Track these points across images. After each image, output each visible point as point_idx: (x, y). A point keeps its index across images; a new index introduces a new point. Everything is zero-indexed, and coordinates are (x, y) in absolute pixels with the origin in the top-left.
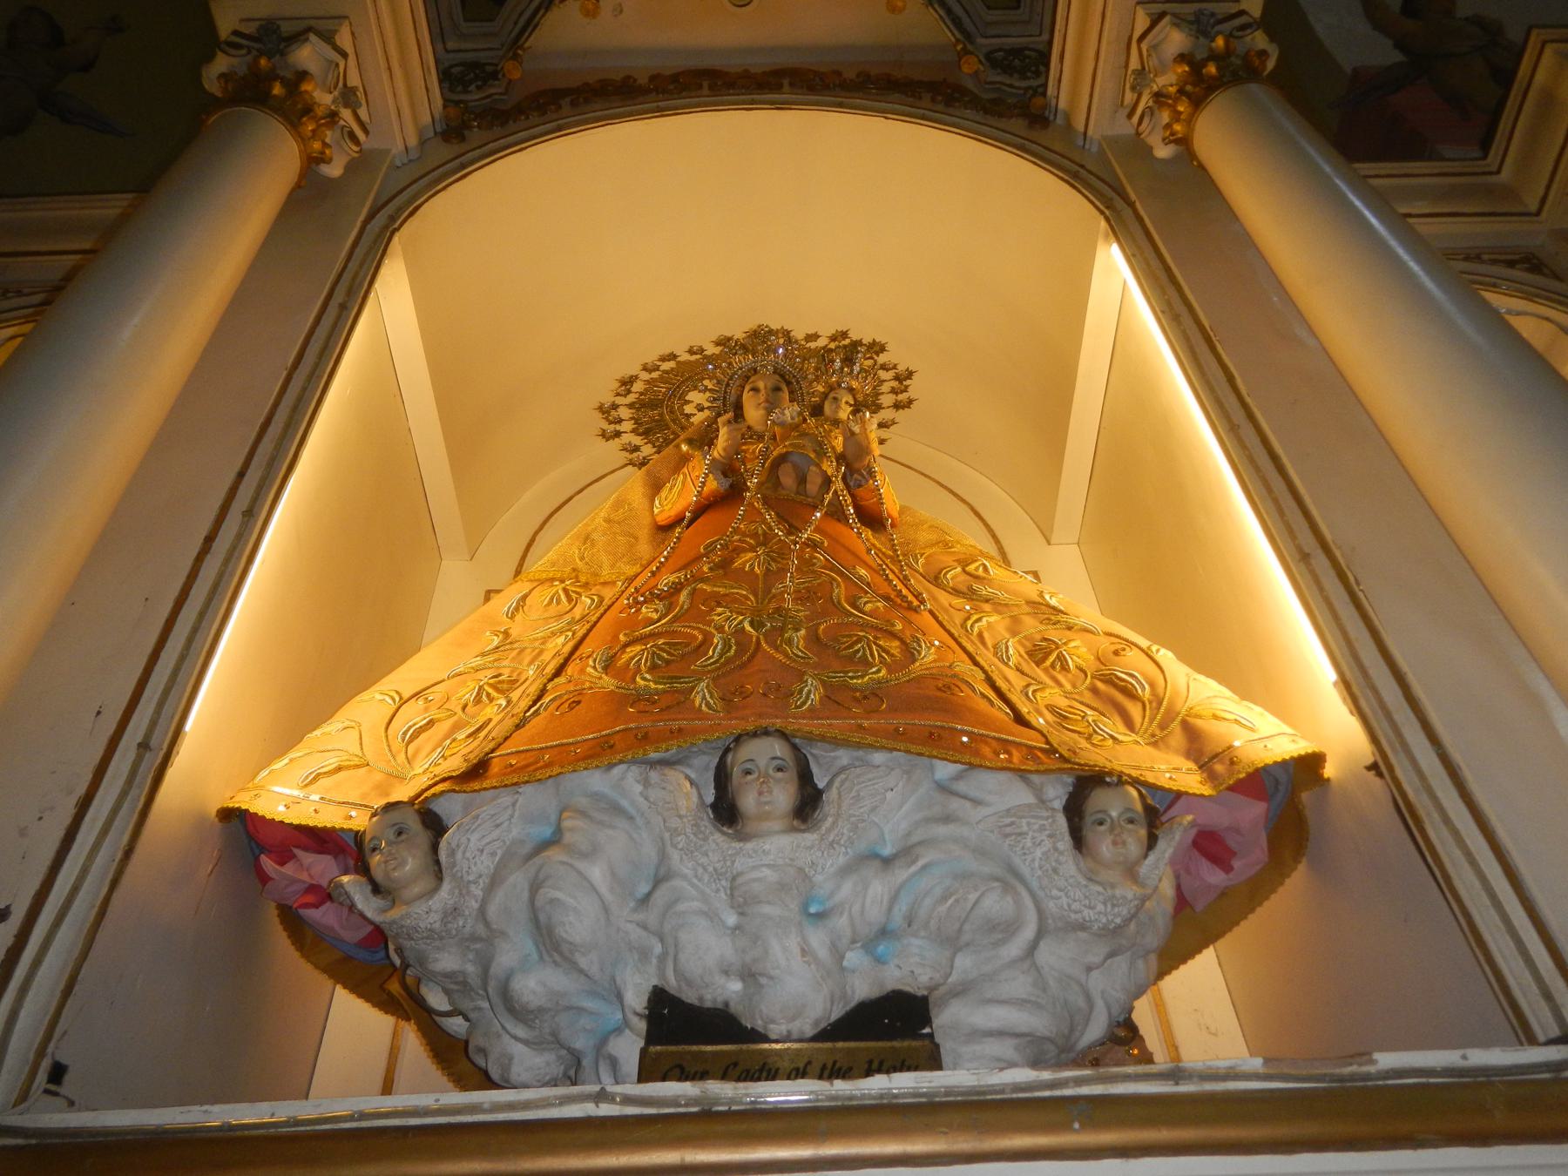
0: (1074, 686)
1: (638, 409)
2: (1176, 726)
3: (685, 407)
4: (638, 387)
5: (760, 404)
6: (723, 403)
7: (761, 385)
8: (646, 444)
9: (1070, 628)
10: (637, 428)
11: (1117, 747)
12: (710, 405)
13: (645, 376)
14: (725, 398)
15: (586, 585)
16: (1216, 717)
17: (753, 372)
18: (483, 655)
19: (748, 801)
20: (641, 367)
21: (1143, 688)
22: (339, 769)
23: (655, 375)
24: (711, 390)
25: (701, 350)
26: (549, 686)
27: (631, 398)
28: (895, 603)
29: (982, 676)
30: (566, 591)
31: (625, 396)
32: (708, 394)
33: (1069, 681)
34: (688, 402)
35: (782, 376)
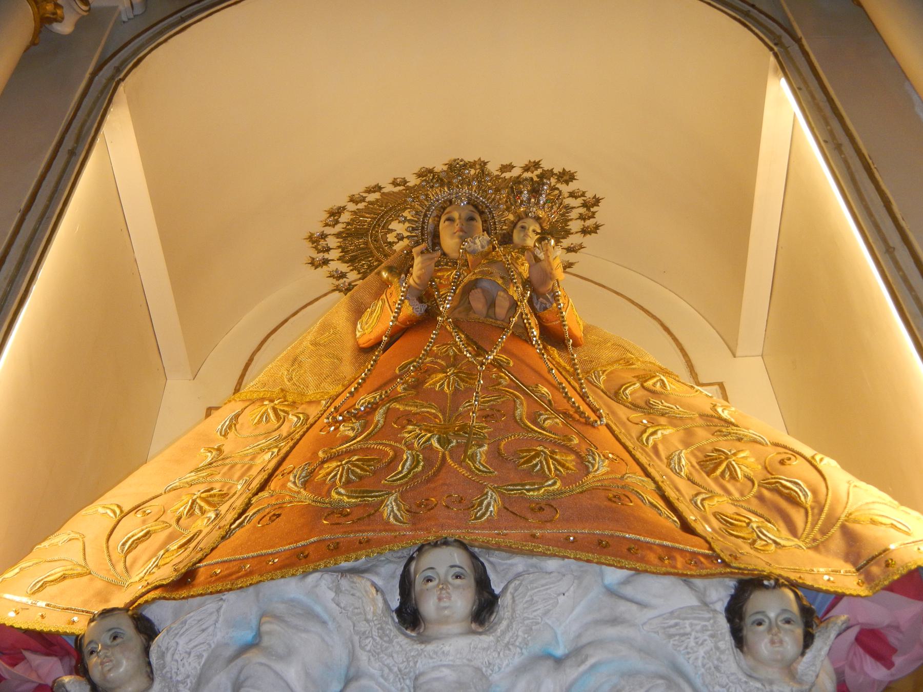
0: (742, 495)
1: (345, 239)
2: (835, 530)
3: (388, 236)
4: (345, 217)
5: (455, 233)
6: (422, 232)
7: (456, 215)
8: (352, 270)
9: (740, 439)
10: (343, 256)
11: (779, 551)
12: (409, 234)
13: (352, 207)
14: (423, 228)
15: (293, 404)
16: (873, 522)
17: (449, 203)
18: (197, 470)
19: (429, 606)
20: (348, 199)
21: (806, 495)
22: (64, 578)
23: (361, 206)
24: (409, 221)
25: (404, 182)
26: (254, 500)
27: (339, 228)
28: (574, 419)
29: (652, 486)
30: (275, 410)
31: (334, 226)
32: (407, 225)
33: (737, 489)
35: (476, 207)
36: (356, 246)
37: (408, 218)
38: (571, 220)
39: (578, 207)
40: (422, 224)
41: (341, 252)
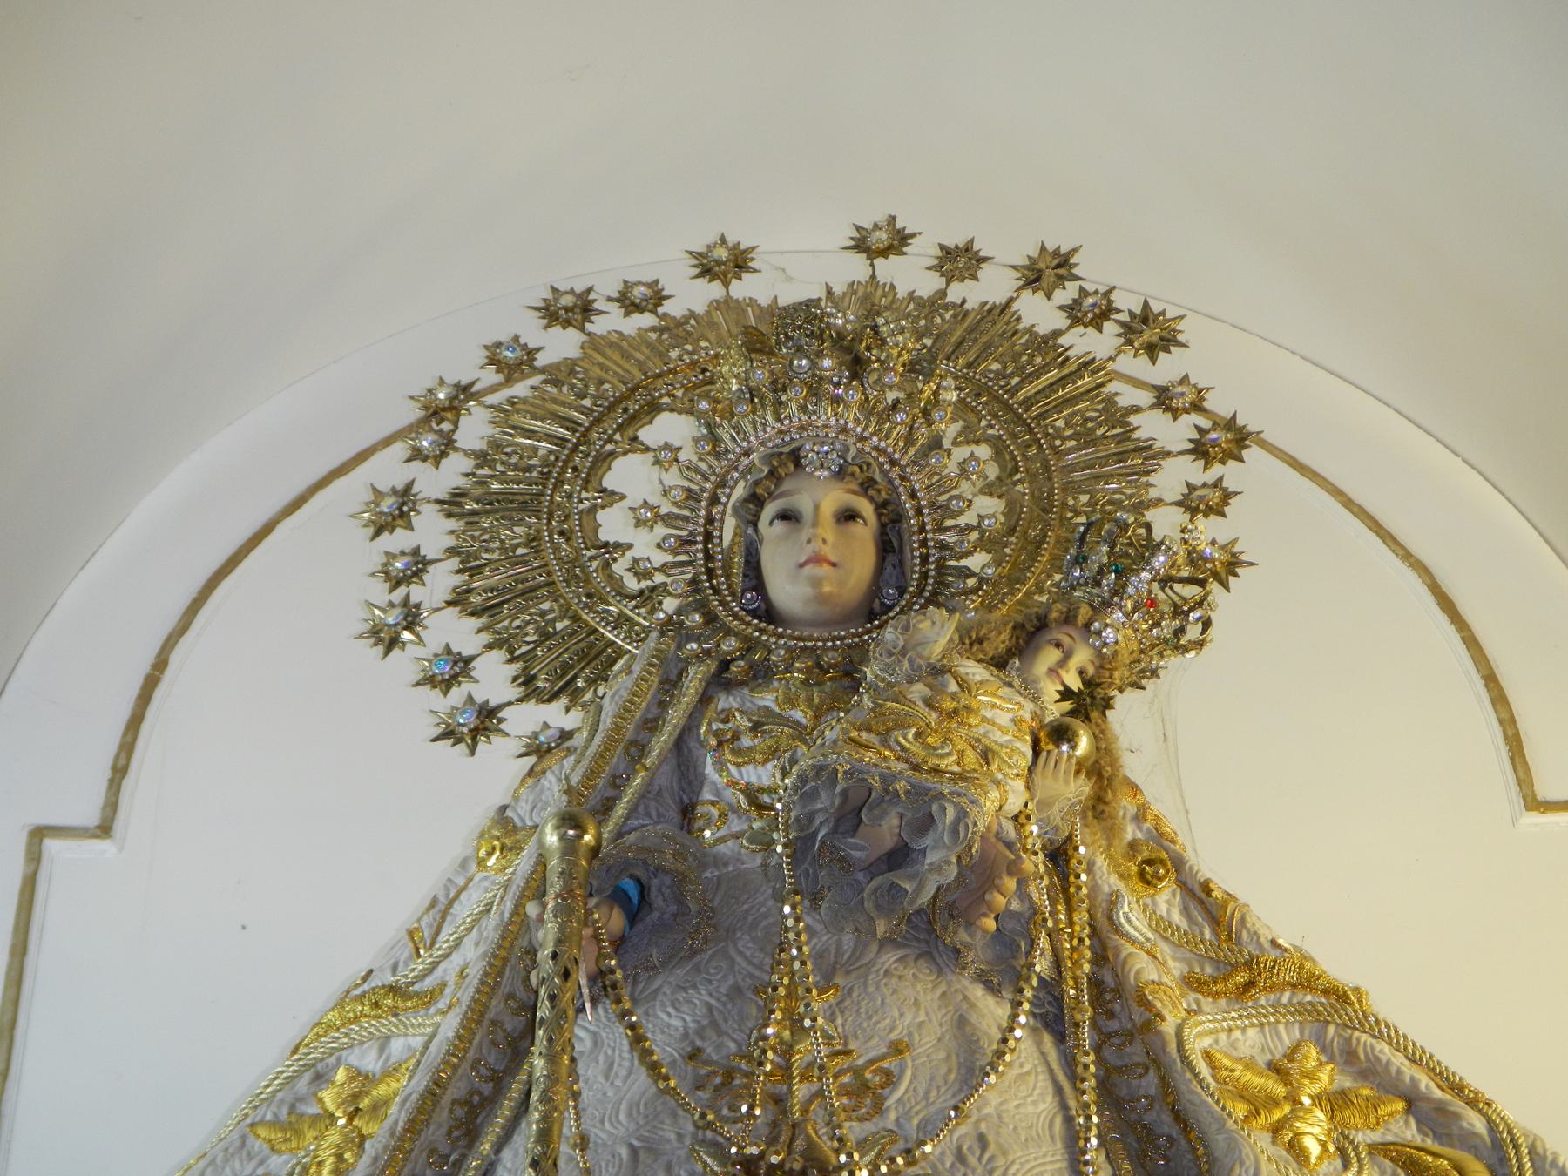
3: (601, 516)
4: (474, 429)
6: (706, 551)
8: (490, 647)
12: (669, 558)
14: (708, 537)
24: (668, 519)
27: (453, 473)
31: (437, 459)
32: (661, 530)
34: (612, 497)
36: (503, 549)
37: (663, 511)
38: (1158, 502)
39: (1181, 453)
40: (705, 526)
41: (459, 572)
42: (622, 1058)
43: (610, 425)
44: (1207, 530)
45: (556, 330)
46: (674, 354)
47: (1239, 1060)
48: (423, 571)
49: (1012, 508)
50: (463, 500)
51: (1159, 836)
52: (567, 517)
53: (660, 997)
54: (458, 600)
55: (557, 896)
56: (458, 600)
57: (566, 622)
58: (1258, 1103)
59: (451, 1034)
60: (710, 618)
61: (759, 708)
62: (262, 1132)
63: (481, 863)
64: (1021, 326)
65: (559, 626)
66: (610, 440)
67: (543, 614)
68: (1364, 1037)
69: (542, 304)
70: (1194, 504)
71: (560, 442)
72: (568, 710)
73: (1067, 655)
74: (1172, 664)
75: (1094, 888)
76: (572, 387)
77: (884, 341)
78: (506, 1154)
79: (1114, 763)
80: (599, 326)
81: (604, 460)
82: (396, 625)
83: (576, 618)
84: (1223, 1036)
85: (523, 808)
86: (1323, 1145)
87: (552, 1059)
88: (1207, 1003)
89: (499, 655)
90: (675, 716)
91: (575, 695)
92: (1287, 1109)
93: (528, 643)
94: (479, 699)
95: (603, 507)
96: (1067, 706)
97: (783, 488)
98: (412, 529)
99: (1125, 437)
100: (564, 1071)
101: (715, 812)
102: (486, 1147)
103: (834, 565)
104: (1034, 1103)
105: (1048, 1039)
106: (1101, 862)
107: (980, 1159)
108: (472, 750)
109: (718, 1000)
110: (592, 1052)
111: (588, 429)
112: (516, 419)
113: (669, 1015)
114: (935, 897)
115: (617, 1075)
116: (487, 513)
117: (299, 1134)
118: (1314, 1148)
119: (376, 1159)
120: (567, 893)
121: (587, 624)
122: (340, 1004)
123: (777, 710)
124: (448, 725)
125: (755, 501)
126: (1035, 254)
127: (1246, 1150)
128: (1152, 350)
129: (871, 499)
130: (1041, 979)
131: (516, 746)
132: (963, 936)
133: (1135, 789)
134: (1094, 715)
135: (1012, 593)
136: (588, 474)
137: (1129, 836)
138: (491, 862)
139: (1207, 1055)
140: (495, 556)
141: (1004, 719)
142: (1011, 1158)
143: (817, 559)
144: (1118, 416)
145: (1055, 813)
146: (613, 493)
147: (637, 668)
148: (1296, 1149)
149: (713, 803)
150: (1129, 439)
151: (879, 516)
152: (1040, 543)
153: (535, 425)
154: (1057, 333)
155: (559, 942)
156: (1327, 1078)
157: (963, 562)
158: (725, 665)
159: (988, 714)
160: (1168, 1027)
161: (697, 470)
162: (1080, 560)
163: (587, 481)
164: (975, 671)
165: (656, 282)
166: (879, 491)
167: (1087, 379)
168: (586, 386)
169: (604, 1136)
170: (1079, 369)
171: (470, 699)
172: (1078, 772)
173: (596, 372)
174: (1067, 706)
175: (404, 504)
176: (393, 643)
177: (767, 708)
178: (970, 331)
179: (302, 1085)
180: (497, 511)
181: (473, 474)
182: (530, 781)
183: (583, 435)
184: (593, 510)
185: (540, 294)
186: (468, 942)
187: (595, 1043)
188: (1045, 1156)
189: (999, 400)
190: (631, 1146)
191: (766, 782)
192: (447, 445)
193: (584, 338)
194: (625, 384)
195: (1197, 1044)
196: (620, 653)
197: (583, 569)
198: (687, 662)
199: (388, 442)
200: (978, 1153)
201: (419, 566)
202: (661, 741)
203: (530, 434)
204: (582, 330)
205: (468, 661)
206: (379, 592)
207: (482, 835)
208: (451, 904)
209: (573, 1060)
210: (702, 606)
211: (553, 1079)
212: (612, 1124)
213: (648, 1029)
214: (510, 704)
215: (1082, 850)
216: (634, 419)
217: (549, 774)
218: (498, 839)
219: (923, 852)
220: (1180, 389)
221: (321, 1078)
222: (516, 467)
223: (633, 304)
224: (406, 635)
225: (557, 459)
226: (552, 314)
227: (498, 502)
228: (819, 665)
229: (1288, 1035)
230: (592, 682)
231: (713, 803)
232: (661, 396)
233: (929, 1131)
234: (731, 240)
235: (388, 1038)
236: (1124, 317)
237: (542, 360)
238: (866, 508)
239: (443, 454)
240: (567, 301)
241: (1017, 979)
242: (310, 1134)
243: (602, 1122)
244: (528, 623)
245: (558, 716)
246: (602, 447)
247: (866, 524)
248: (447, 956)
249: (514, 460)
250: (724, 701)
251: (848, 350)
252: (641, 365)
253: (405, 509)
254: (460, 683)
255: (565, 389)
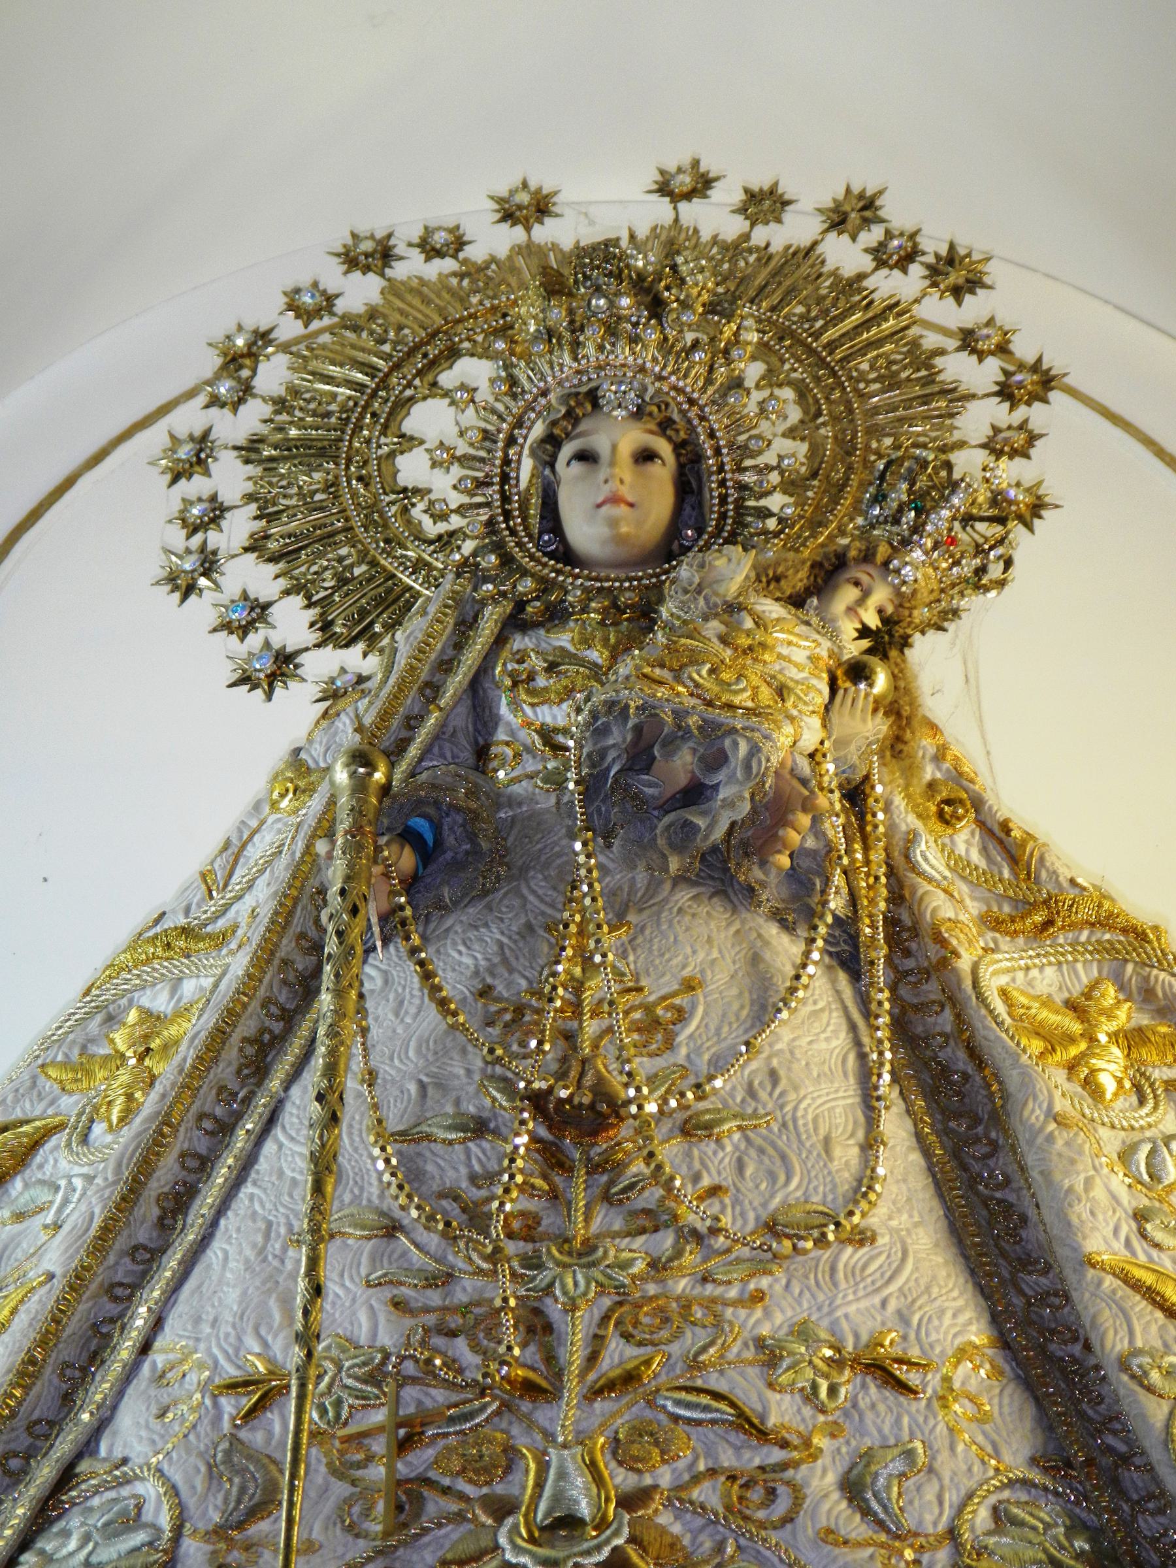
3: (400, 461)
6: (502, 492)
8: (287, 593)
12: (465, 499)
14: (505, 478)
24: (464, 460)
31: (236, 405)
32: (457, 471)
36: (301, 495)
37: (458, 453)
40: (501, 467)
41: (256, 518)
42: (412, 996)
43: (409, 370)
44: (1008, 471)
45: (357, 275)
46: (474, 300)
47: (1037, 998)
48: (221, 517)
49: (815, 451)
50: (260, 446)
51: (958, 776)
52: (366, 462)
53: (451, 935)
54: (255, 546)
55: (346, 833)
56: (255, 546)
57: (364, 568)
58: (1054, 1040)
59: (240, 973)
60: (507, 560)
61: (555, 648)
62: (53, 1073)
63: (274, 805)
64: (825, 270)
65: (357, 571)
66: (409, 385)
67: (340, 560)
68: (1163, 975)
69: (342, 250)
70: (997, 446)
71: (360, 387)
72: (365, 655)
73: (866, 594)
74: (972, 602)
75: (891, 827)
76: (371, 333)
77: (683, 281)
78: (295, 1091)
79: (913, 703)
80: (399, 271)
81: (403, 405)
82: (193, 571)
83: (373, 563)
84: (1020, 975)
85: (317, 750)
86: (1120, 1082)
87: (339, 994)
88: (1004, 942)
89: (298, 600)
90: (471, 658)
91: (373, 641)
92: (1083, 1046)
93: (326, 589)
94: (276, 645)
95: (402, 453)
96: (865, 643)
97: (582, 427)
98: (210, 476)
99: (929, 381)
100: (351, 1007)
101: (509, 752)
102: (274, 1084)
103: (631, 505)
104: (827, 1039)
105: (842, 977)
106: (899, 801)
107: (771, 1094)
108: (269, 696)
109: (510, 938)
110: (382, 990)
111: (387, 375)
112: (314, 365)
113: (460, 953)
114: (730, 832)
115: (407, 1013)
116: (285, 459)
117: (90, 1074)
118: (1108, 1083)
119: (164, 1096)
120: (356, 830)
121: (385, 569)
122: (132, 947)
123: (572, 649)
124: (244, 671)
125: (552, 442)
126: (840, 196)
127: (1040, 1085)
128: (957, 293)
129: (669, 439)
130: (835, 916)
131: (314, 691)
132: (757, 873)
133: (934, 728)
134: (893, 653)
135: (814, 535)
136: (387, 420)
137: (928, 776)
138: (284, 804)
139: (1004, 993)
140: (293, 502)
141: (800, 656)
142: (802, 1093)
143: (615, 499)
144: (924, 360)
145: (853, 754)
146: (412, 438)
147: (432, 609)
148: (1091, 1085)
149: (507, 744)
150: (933, 382)
151: (678, 455)
152: (842, 486)
153: (334, 370)
154: (861, 276)
155: (348, 879)
156: (1125, 1016)
157: (763, 502)
158: (520, 605)
159: (784, 651)
160: (964, 964)
161: (494, 411)
162: (880, 498)
163: (385, 427)
164: (772, 609)
165: (458, 227)
166: (677, 431)
167: (892, 322)
168: (386, 331)
169: (393, 1072)
170: (884, 312)
171: (267, 644)
172: (875, 710)
173: (396, 317)
174: (865, 643)
175: (201, 450)
176: (189, 590)
177: (562, 649)
178: (775, 273)
179: (94, 1025)
180: (295, 457)
181: (271, 421)
182: (324, 723)
183: (383, 380)
184: (392, 455)
185: (340, 238)
186: (261, 883)
187: (386, 982)
188: (837, 1091)
189: (803, 343)
190: (420, 1082)
191: (561, 722)
192: (246, 391)
193: (384, 283)
194: (425, 329)
195: (992, 983)
196: (417, 595)
197: (382, 514)
198: (483, 603)
199: (191, 394)
200: (769, 1088)
201: (216, 512)
202: (456, 682)
203: (329, 379)
204: (382, 275)
205: (265, 607)
206: (177, 537)
207: (275, 778)
208: (244, 846)
209: (361, 996)
210: (499, 548)
211: (340, 1013)
212: (401, 1061)
213: (438, 965)
214: (307, 649)
215: (879, 789)
216: (433, 364)
217: (343, 716)
218: (291, 781)
219: (716, 787)
220: (985, 331)
221: (111, 1020)
222: (314, 414)
223: (433, 249)
224: (203, 582)
225: (356, 404)
226: (352, 261)
227: (297, 448)
228: (614, 605)
229: (1085, 974)
230: (390, 627)
231: (507, 744)
232: (461, 341)
233: (719, 1065)
234: (533, 185)
235: (180, 979)
236: (930, 259)
237: (341, 306)
238: (664, 448)
239: (241, 401)
240: (367, 246)
241: (811, 916)
242: (101, 1074)
243: (392, 1059)
244: (326, 568)
245: (355, 659)
246: (401, 392)
247: (664, 463)
248: (239, 898)
249: (312, 406)
250: (519, 642)
251: (648, 291)
252: (441, 311)
253: (203, 455)
254: (257, 629)
255: (364, 335)
